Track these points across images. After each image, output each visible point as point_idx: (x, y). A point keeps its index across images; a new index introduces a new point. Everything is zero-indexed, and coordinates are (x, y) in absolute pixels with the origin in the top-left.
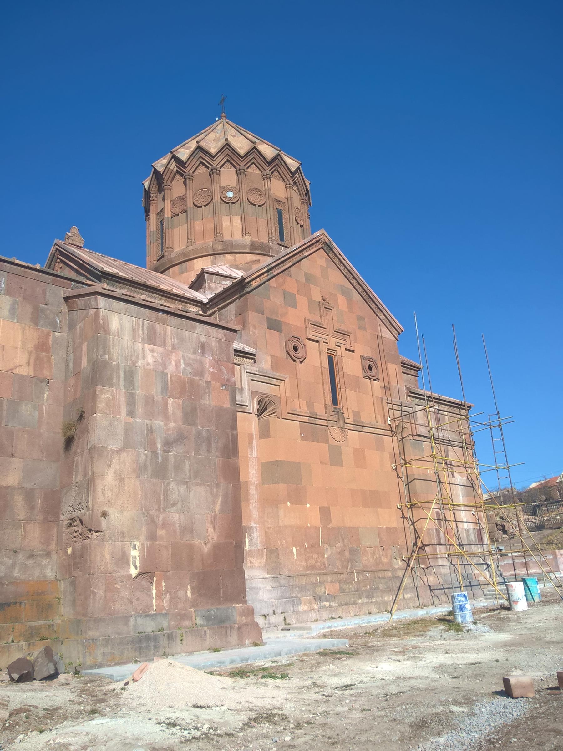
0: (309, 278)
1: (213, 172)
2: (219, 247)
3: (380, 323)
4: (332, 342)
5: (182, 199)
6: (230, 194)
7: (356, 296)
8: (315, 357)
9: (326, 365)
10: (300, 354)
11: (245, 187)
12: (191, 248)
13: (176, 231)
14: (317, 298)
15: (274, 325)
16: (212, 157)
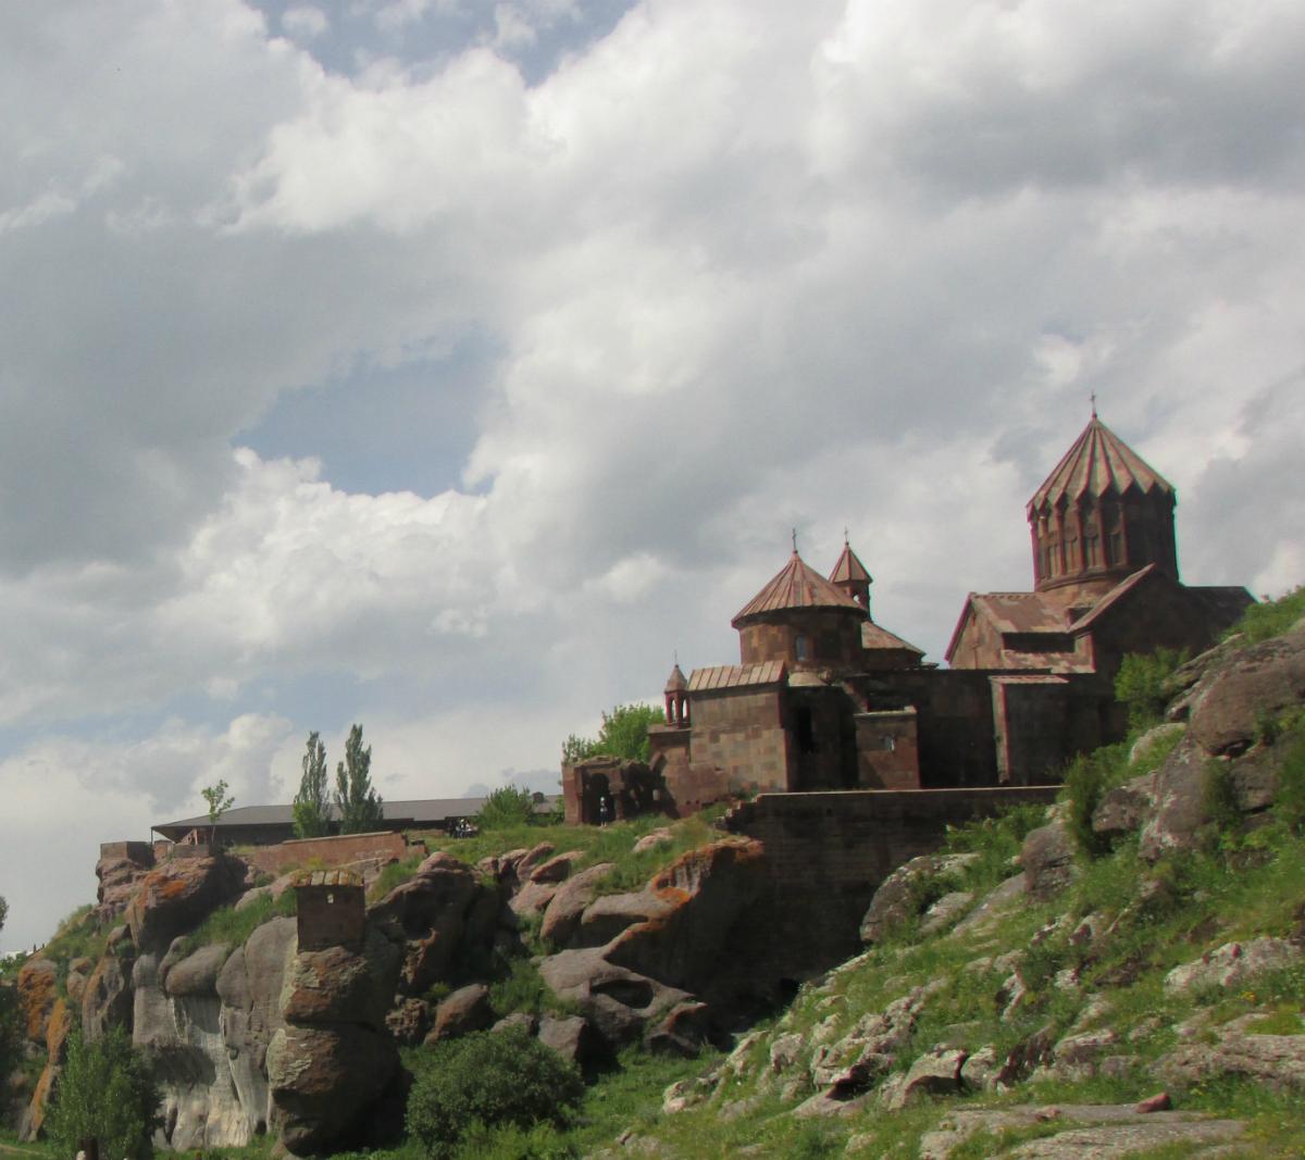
12: (1063, 577)
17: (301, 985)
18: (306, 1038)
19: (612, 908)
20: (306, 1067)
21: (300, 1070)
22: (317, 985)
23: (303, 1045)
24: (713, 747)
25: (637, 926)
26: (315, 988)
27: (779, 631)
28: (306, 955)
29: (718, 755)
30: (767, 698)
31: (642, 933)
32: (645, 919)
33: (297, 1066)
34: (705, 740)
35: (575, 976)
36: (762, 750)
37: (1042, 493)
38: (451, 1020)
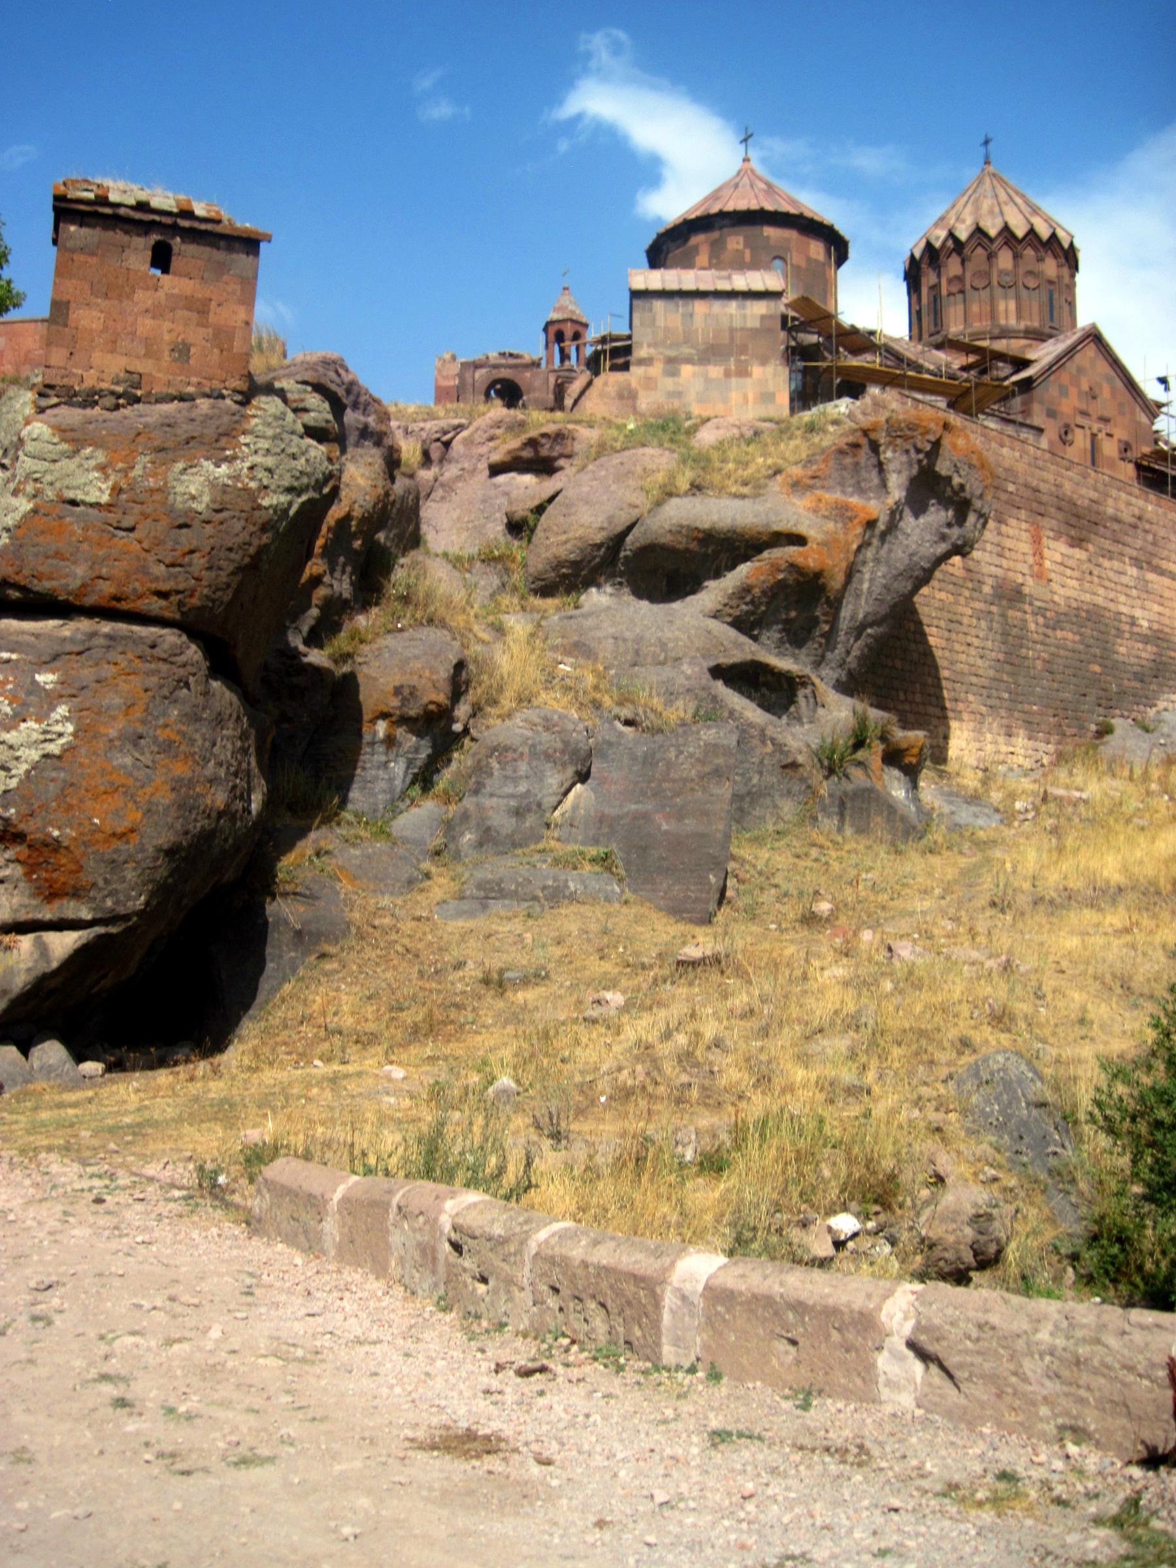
0: (1080, 370)
1: (991, 256)
2: (996, 332)
3: (1138, 409)
4: (1096, 427)
5: (960, 279)
6: (1008, 279)
7: (1119, 384)
8: (1081, 440)
9: (1089, 446)
10: (1070, 437)
11: (1021, 271)
13: (952, 310)
14: (1085, 387)
15: (1051, 414)
16: (991, 240)
17: (50, 494)
18: (56, 657)
19: (715, 517)
20: (54, 748)
21: (34, 755)
22: (105, 498)
23: (46, 678)
24: (668, 383)
25: (791, 552)
26: (96, 505)
27: (745, 246)
28: (71, 415)
29: (678, 394)
30: (763, 317)
31: (792, 566)
32: (799, 540)
33: (28, 742)
34: (656, 370)
35: (663, 645)
36: (751, 396)
37: (943, 234)
38: (395, 702)
